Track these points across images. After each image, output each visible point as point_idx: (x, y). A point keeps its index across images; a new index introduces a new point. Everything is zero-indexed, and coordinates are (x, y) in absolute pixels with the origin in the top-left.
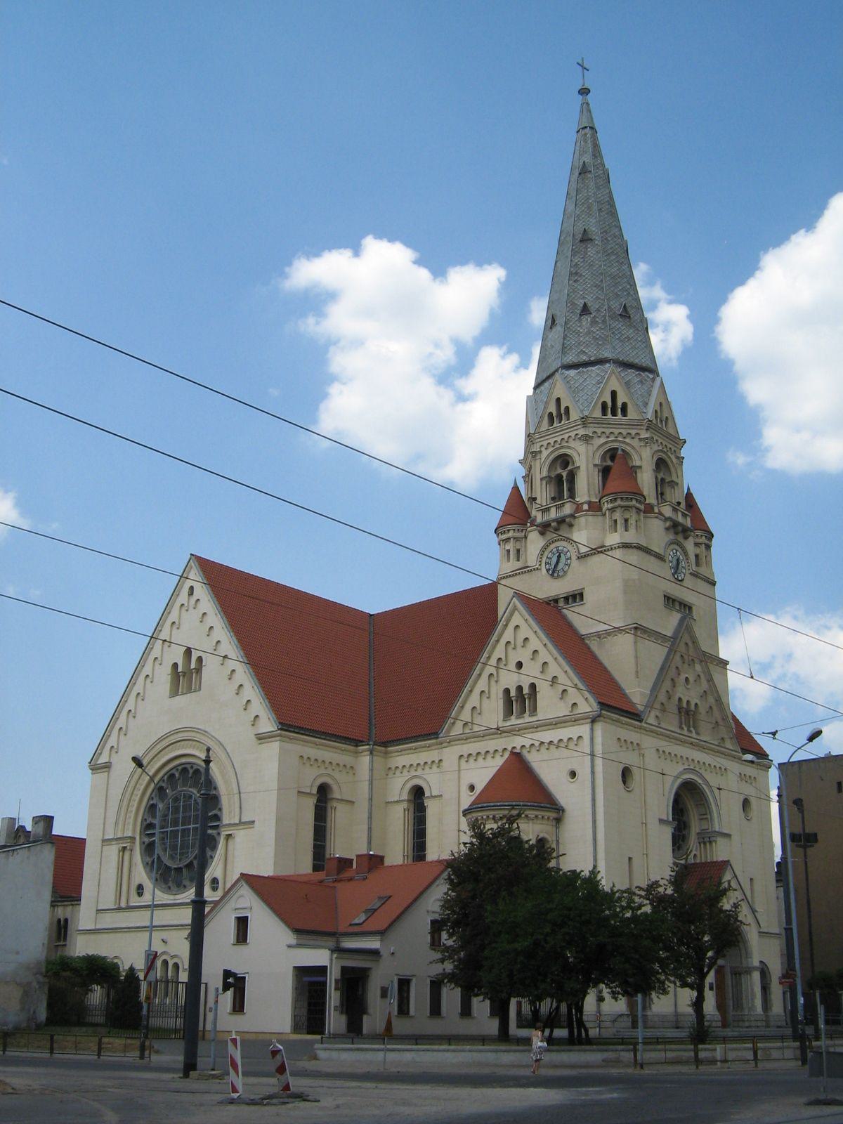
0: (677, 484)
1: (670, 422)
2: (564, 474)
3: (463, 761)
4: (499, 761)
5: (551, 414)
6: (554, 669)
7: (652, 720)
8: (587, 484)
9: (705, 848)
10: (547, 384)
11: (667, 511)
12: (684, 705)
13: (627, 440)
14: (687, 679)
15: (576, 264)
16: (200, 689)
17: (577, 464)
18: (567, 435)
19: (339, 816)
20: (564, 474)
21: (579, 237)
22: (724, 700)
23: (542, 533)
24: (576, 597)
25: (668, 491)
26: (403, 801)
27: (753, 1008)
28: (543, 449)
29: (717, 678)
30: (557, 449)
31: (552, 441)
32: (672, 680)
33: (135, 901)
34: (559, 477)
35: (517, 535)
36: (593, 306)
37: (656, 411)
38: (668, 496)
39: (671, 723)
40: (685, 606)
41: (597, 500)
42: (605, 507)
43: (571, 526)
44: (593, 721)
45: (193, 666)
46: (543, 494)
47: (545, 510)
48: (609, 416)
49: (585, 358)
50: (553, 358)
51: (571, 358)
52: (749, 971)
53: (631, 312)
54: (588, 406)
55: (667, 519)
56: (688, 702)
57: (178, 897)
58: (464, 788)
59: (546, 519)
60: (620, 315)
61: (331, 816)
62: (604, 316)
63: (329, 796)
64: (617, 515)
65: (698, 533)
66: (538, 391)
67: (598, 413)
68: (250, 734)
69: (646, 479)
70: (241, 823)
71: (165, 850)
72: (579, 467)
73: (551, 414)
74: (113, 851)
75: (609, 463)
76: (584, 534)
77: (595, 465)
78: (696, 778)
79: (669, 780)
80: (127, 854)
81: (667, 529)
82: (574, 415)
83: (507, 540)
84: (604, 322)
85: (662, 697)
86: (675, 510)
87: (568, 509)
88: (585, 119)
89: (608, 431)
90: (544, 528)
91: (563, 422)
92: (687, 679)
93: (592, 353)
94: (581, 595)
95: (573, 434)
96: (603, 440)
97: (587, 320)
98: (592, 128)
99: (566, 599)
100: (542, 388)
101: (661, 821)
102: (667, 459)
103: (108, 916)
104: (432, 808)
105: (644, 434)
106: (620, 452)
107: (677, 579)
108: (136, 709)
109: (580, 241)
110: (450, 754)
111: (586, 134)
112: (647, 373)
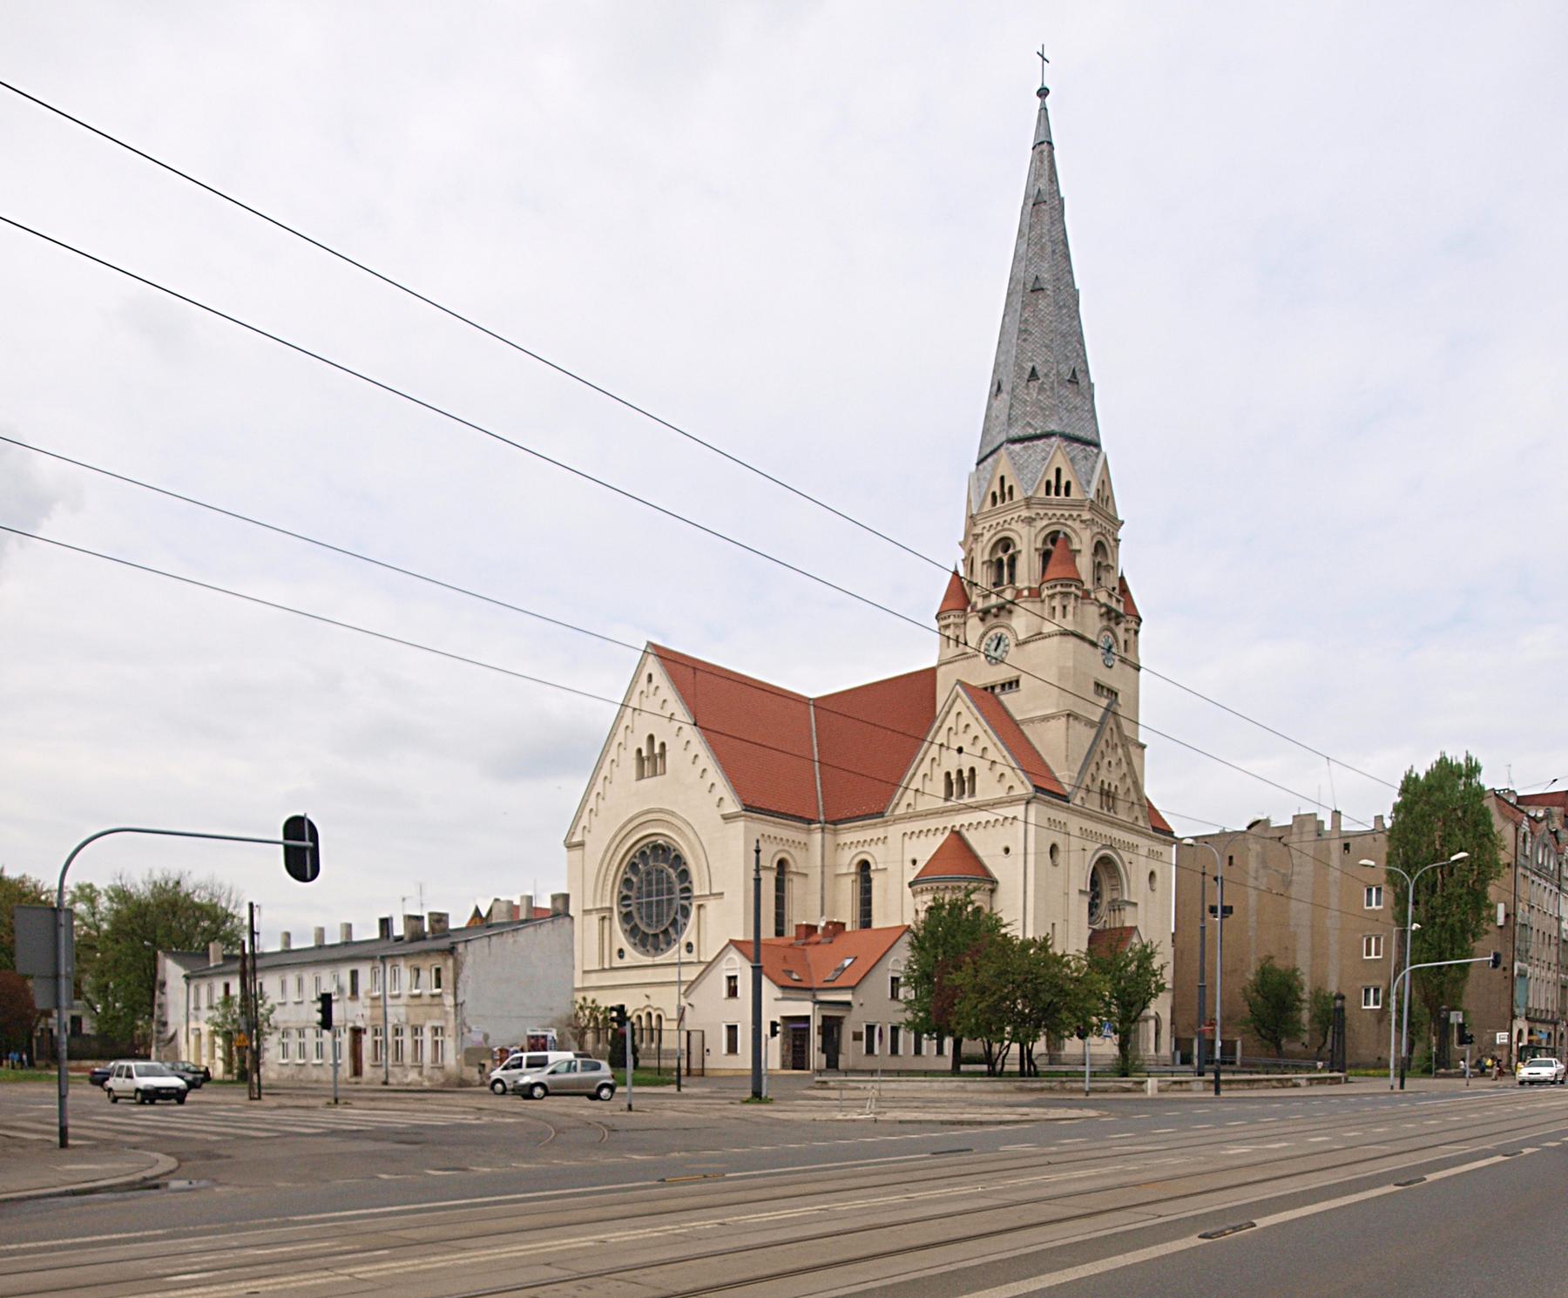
0: (1112, 568)
1: (1110, 501)
2: (1005, 559)
3: (906, 838)
4: (940, 840)
5: (994, 494)
6: (992, 754)
7: (1078, 801)
8: (1027, 570)
9: (1115, 918)
10: (990, 460)
11: (1103, 597)
12: (1106, 787)
13: (1069, 522)
14: (1110, 762)
15: (1026, 320)
16: (664, 773)
17: (1018, 548)
18: (1010, 517)
19: (794, 887)
20: (1005, 559)
21: (1029, 286)
22: (1140, 781)
23: (982, 620)
24: (1013, 684)
25: (1103, 575)
26: (851, 874)
27: (1147, 1049)
28: (985, 531)
29: (1135, 761)
30: (999, 532)
31: (994, 523)
32: (1097, 764)
33: (617, 963)
34: (1000, 561)
35: (957, 620)
36: (1040, 372)
37: (1098, 490)
38: (1103, 582)
39: (1094, 804)
40: (1112, 692)
41: (1037, 586)
42: (1045, 593)
43: (1010, 612)
44: (1028, 803)
45: (657, 750)
46: (983, 577)
47: (986, 597)
48: (1053, 495)
49: (1031, 431)
50: (998, 429)
51: (1016, 432)
52: (1146, 1020)
53: (1080, 376)
54: (1033, 485)
55: (1102, 605)
56: (1109, 784)
57: (656, 958)
58: (909, 864)
59: (987, 605)
60: (1069, 381)
61: (788, 886)
62: (1053, 383)
63: (786, 870)
64: (1056, 602)
65: (1129, 618)
66: (981, 467)
67: (1042, 493)
68: (716, 814)
69: (1084, 564)
70: (711, 894)
71: (641, 918)
72: (1020, 552)
73: (994, 494)
74: (594, 919)
75: (1050, 546)
76: (1021, 623)
77: (1036, 550)
78: (1115, 856)
79: (1089, 854)
80: (607, 923)
81: (1101, 615)
82: (1017, 496)
83: (947, 626)
84: (1052, 389)
85: (1088, 780)
86: (1110, 596)
87: (1008, 595)
88: (1042, 131)
89: (1050, 513)
90: (985, 614)
91: (1006, 502)
92: (1110, 762)
93: (1039, 426)
94: (1017, 682)
95: (1016, 516)
96: (1045, 522)
97: (1034, 385)
98: (1050, 143)
99: (1003, 686)
100: (985, 463)
101: (1081, 892)
102: (1106, 543)
103: (594, 976)
104: (877, 881)
105: (1086, 516)
106: (1061, 536)
107: (1107, 666)
108: (604, 790)
109: (1032, 291)
110: (895, 831)
111: (1042, 152)
112: (1092, 448)
